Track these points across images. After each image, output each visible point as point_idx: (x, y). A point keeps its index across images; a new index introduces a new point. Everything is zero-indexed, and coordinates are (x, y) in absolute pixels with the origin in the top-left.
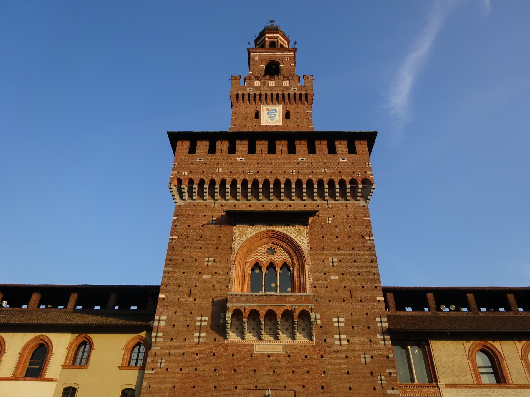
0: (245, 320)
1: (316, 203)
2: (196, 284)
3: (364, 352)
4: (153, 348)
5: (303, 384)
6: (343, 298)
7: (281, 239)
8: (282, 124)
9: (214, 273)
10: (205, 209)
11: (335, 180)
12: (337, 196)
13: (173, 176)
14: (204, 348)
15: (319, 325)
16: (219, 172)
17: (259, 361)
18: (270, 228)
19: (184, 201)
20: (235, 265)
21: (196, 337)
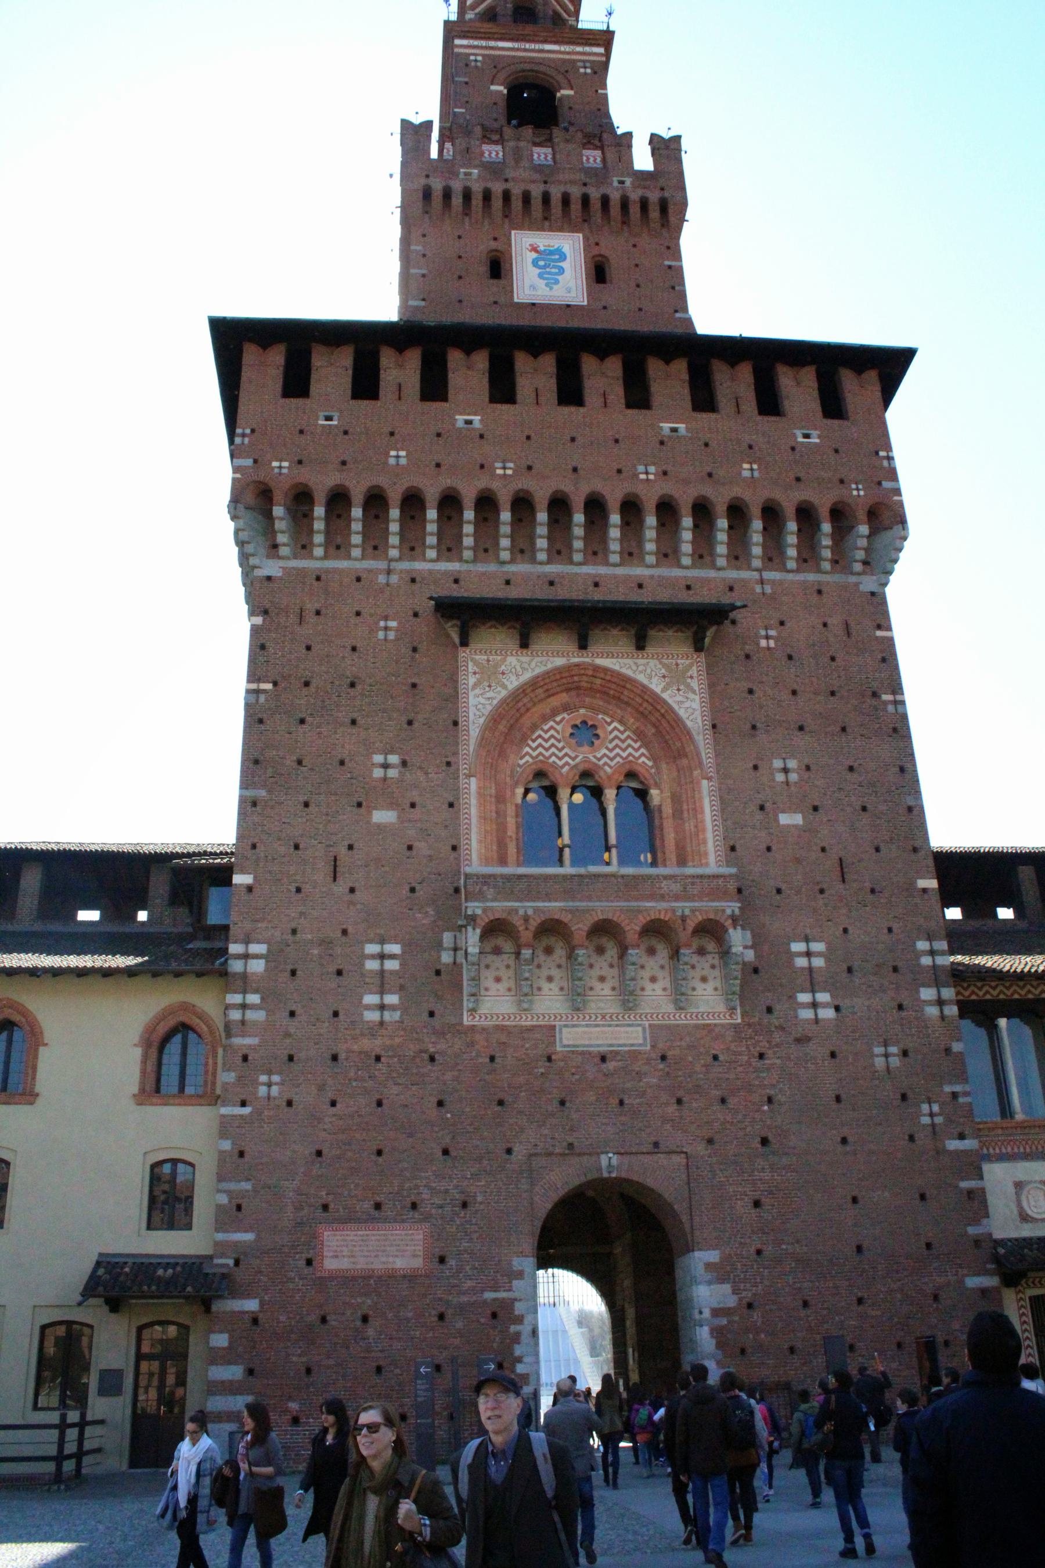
1: (724, 579)
2: (350, 842)
3: (881, 1040)
7: (617, 695)
8: (585, 303)
11: (784, 504)
13: (238, 476)
14: (397, 1040)
15: (750, 963)
18: (579, 657)
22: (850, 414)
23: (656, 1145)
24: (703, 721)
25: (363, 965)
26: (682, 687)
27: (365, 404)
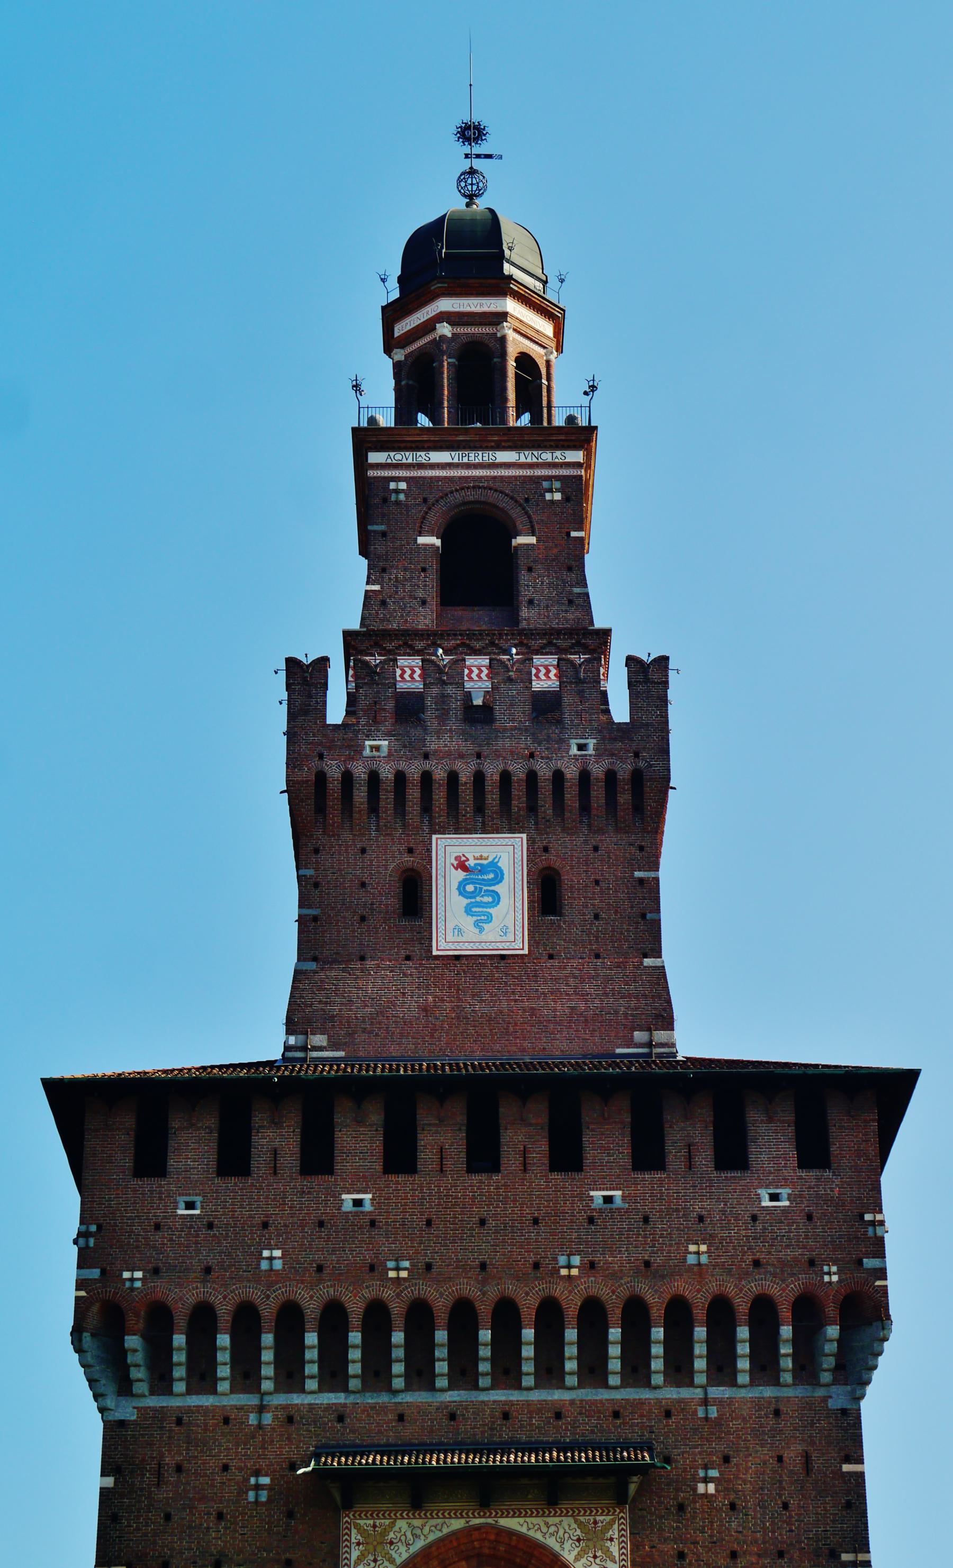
1: (659, 1401)
10: (223, 1434)
13: (83, 1293)
18: (480, 1517)
26: (599, 1554)
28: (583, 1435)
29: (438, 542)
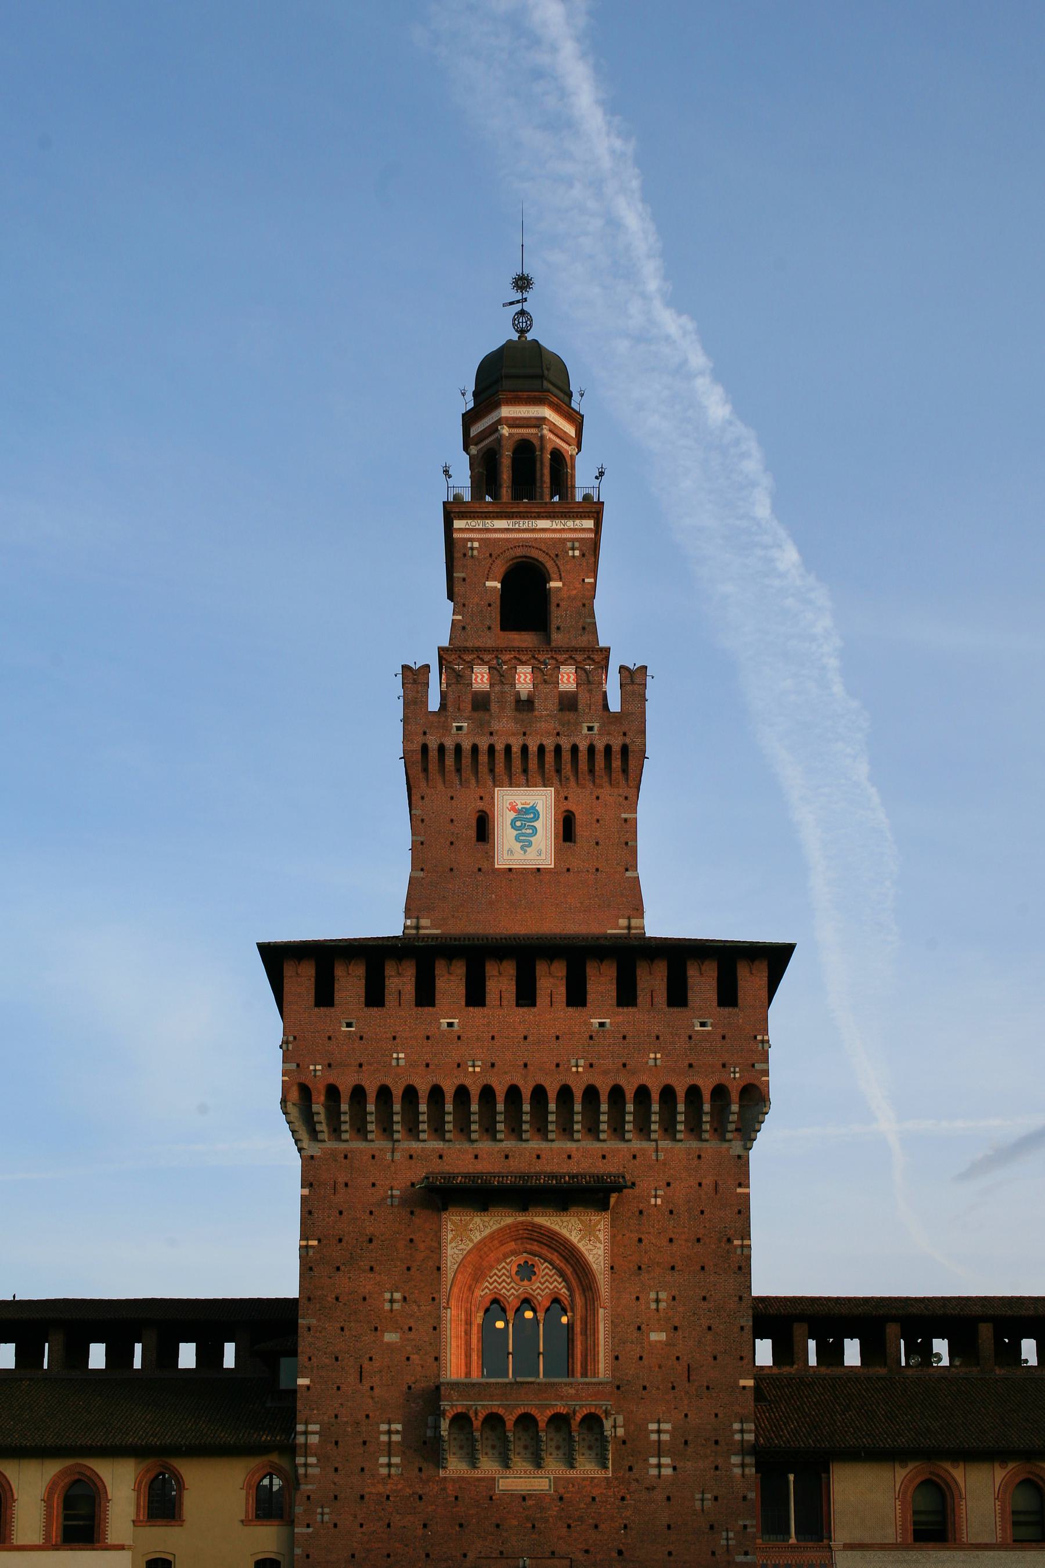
0: (477, 1434)
1: (629, 1149)
2: (370, 1355)
3: (701, 1490)
4: (303, 1487)
5: (586, 1548)
6: (672, 1383)
9: (407, 1327)
12: (680, 1131)
14: (400, 1486)
15: (620, 1437)
16: (398, 1065)
17: (504, 1508)
19: (320, 1145)
20: (449, 1310)
21: (382, 1464)
22: (739, 1001)
23: (553, 1553)
24: (604, 1264)
25: (379, 1438)
26: (592, 1238)
27: (374, 1011)
28: (584, 1169)
29: (499, 586)
